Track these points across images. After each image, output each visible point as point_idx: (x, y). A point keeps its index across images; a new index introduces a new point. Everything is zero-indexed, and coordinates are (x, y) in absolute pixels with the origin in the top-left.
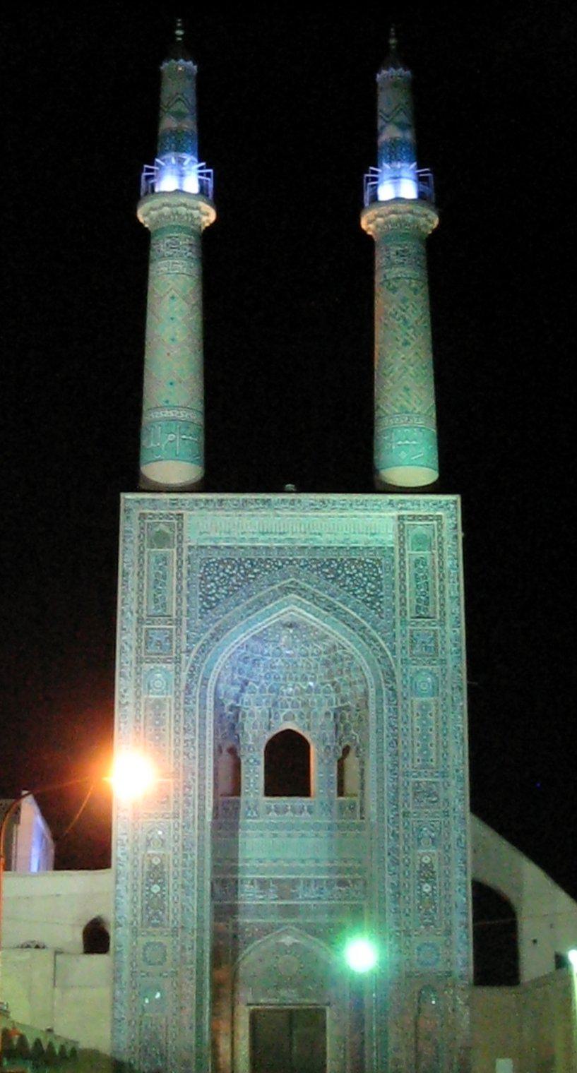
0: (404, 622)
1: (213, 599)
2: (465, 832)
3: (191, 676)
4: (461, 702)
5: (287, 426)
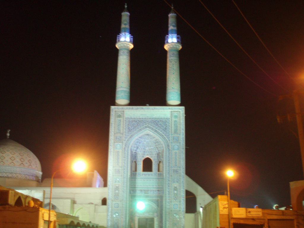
0: (172, 134)
2: (184, 180)
4: (184, 151)
5: (148, 92)
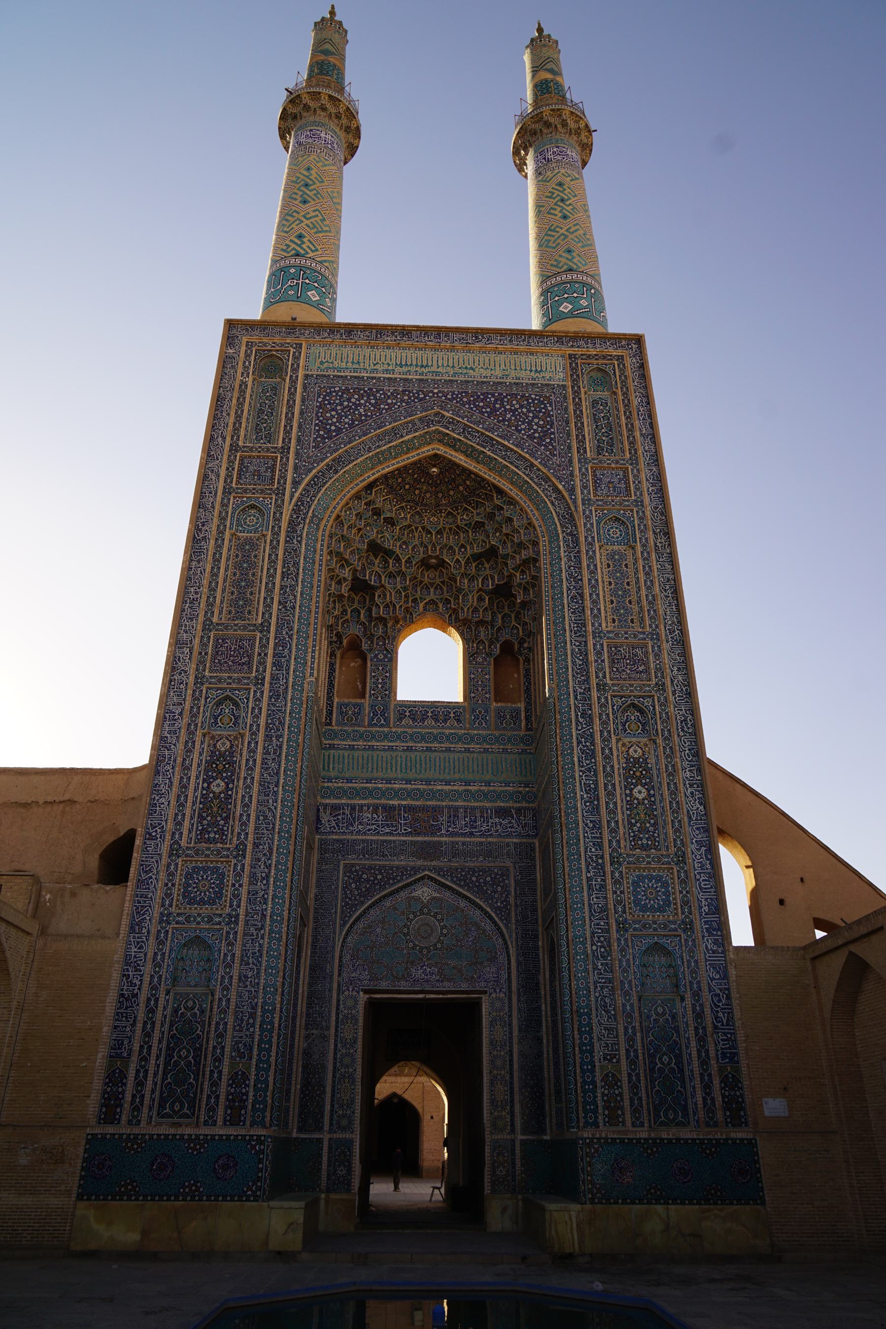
0: (583, 461)
1: (333, 428)
3: (297, 510)
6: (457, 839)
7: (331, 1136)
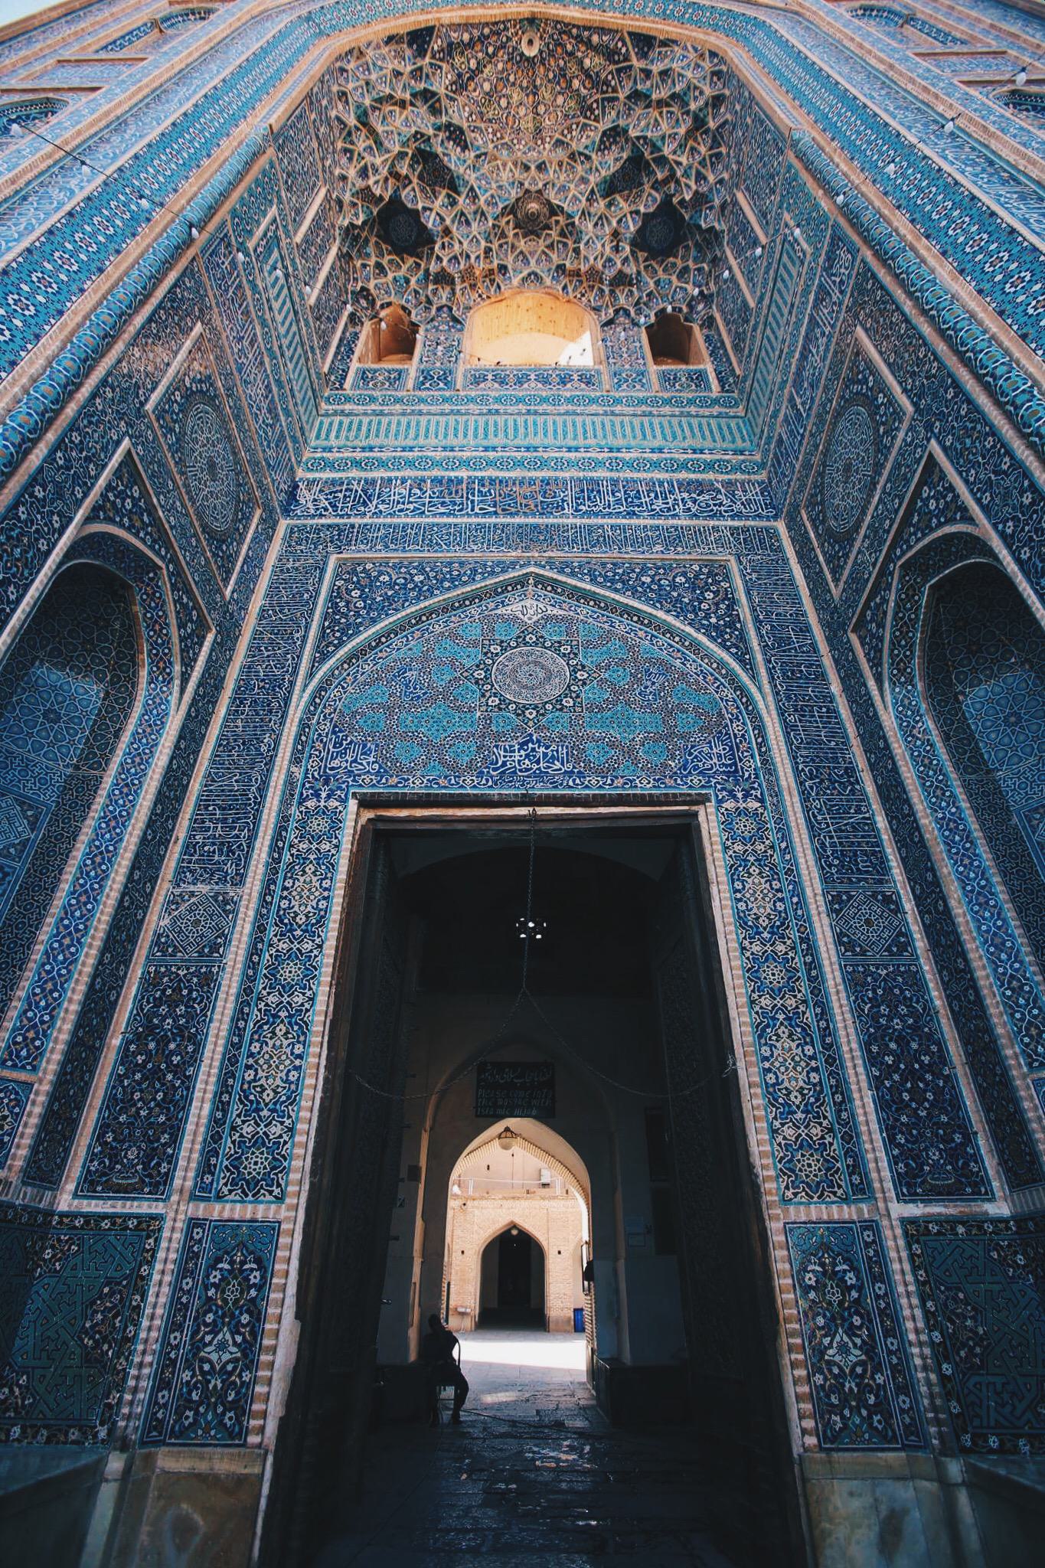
6: (600, 521)
7: (200, 1210)
